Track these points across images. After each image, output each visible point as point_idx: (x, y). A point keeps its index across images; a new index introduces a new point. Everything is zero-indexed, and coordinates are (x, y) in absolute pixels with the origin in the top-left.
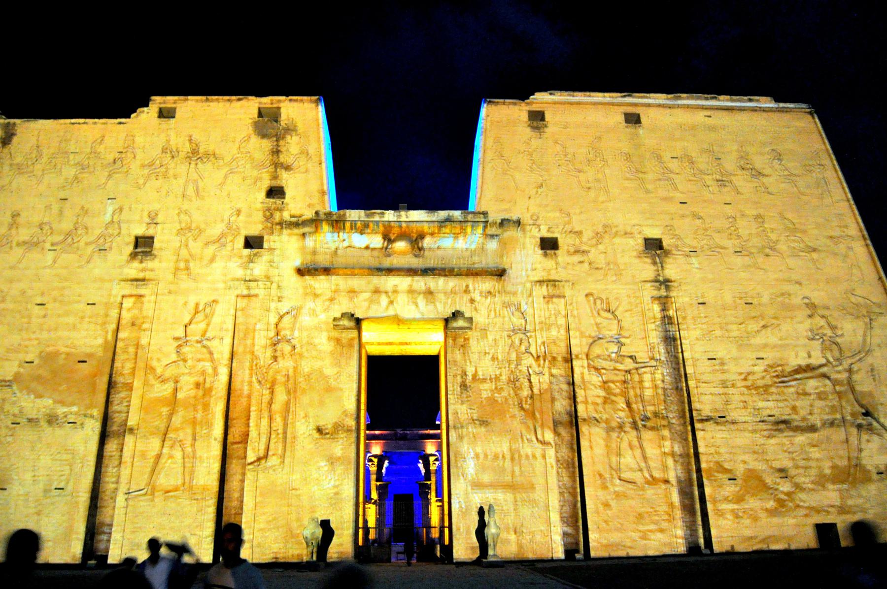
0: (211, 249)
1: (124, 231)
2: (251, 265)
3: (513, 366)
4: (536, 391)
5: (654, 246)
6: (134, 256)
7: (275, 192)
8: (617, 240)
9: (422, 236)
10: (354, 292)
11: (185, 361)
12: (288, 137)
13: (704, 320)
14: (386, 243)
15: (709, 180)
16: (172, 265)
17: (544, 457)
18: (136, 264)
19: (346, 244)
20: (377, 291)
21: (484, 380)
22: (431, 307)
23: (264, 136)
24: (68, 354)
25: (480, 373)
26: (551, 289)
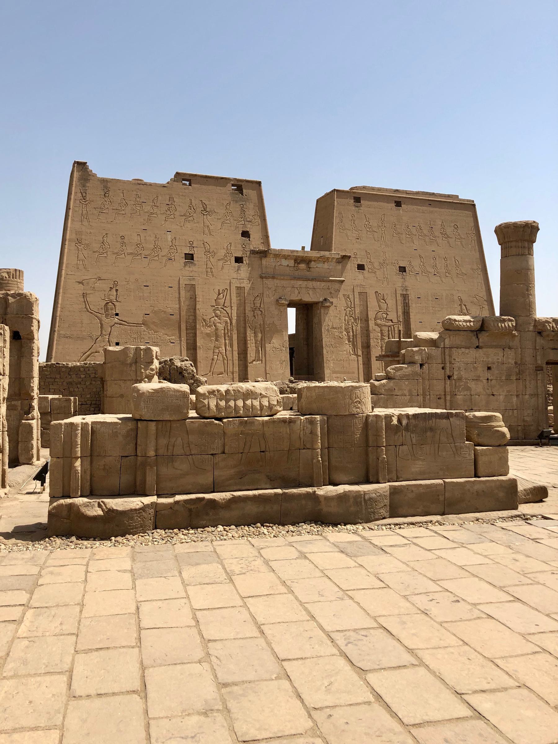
0: (221, 263)
1: (179, 251)
5: (403, 269)
6: (185, 264)
7: (245, 234)
8: (388, 267)
9: (310, 261)
11: (217, 317)
12: (248, 203)
13: (420, 305)
15: (427, 239)
16: (205, 270)
18: (187, 268)
20: (293, 287)
23: (236, 202)
24: (165, 312)
26: (362, 289)
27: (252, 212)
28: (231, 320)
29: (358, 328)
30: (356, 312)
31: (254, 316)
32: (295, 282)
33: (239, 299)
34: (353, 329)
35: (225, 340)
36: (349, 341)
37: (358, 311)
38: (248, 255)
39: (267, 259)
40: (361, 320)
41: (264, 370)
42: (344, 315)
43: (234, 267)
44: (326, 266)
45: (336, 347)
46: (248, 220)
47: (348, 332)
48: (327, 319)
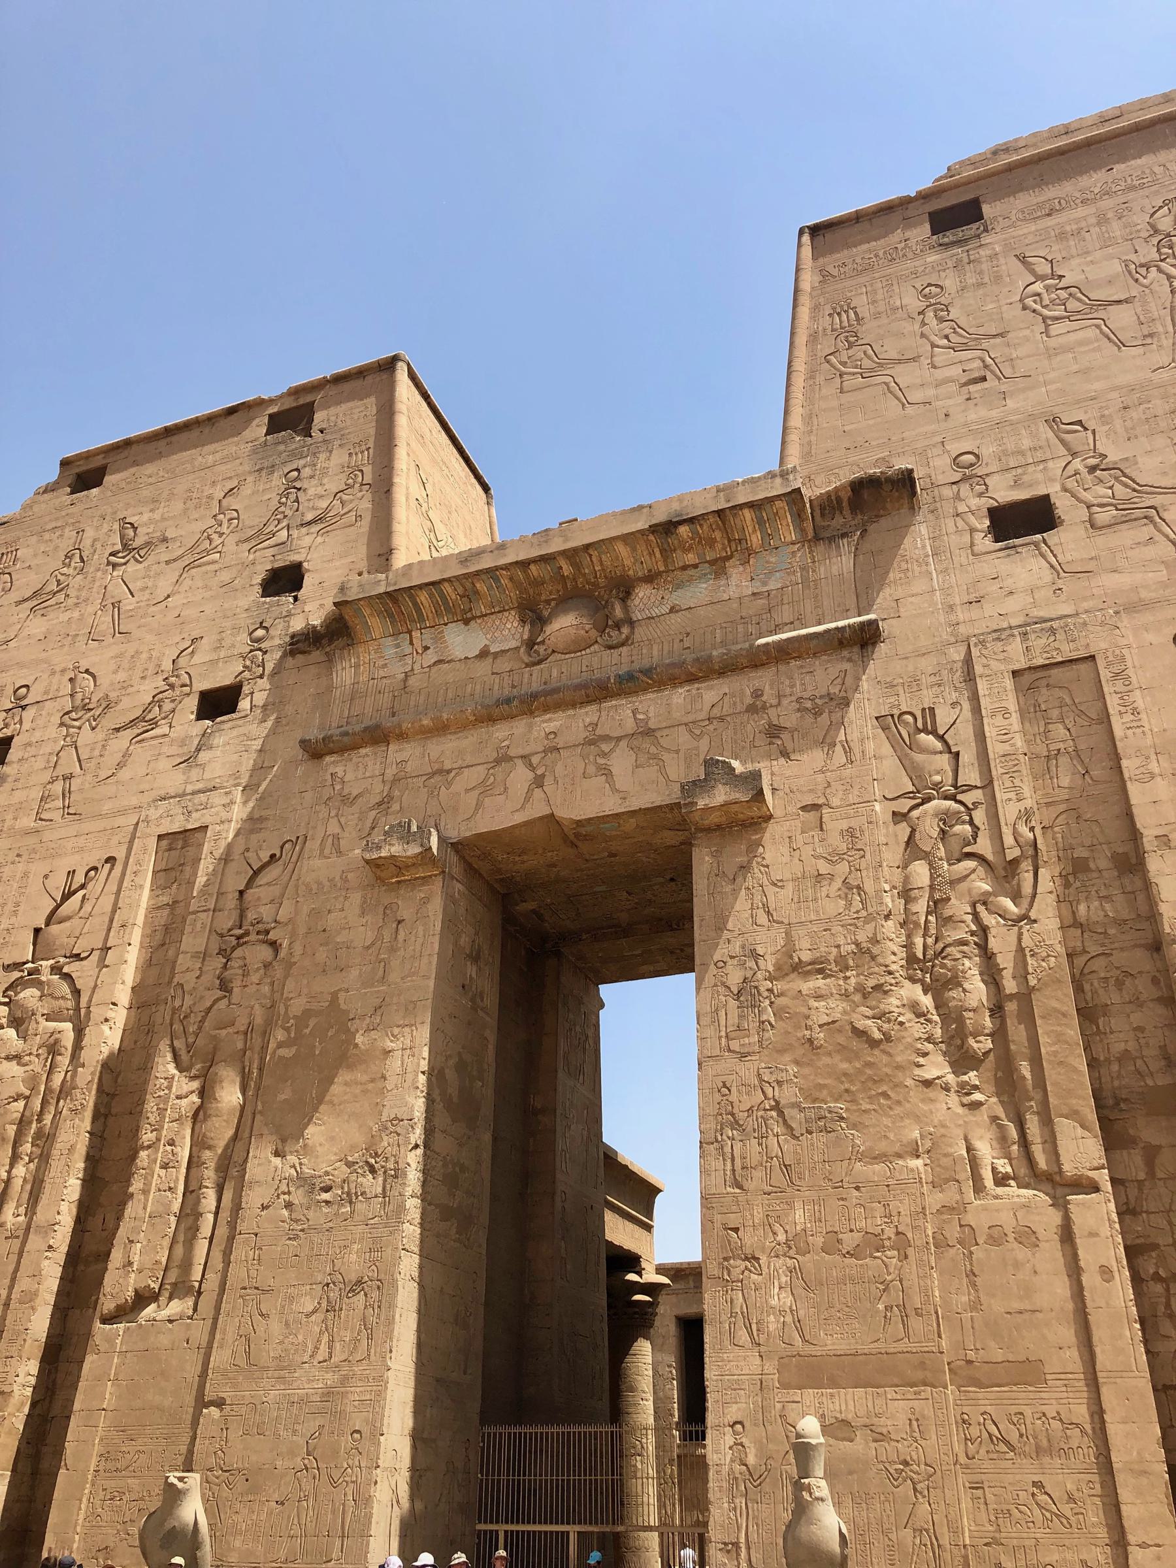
2: (203, 756)
3: (921, 906)
4: (1010, 985)
9: (624, 588)
10: (440, 772)
12: (322, 456)
14: (527, 628)
16: (36, 794)
17: (1067, 1235)
19: (431, 657)
21: (818, 968)
22: (651, 772)
23: (272, 469)
25: (805, 943)
26: (1038, 642)
27: (333, 484)
28: (79, 1033)
29: (1039, 931)
30: (1009, 812)
31: (225, 986)
32: (519, 726)
33: (165, 899)
34: (988, 956)
35: (15, 1158)
36: (962, 1060)
37: (1019, 801)
38: (269, 666)
39: (364, 654)
40: (1076, 870)
41: (192, 1371)
42: (893, 855)
43: (183, 743)
44: (739, 582)
45: (823, 1124)
46: (309, 517)
47: (941, 986)
48: (742, 904)
